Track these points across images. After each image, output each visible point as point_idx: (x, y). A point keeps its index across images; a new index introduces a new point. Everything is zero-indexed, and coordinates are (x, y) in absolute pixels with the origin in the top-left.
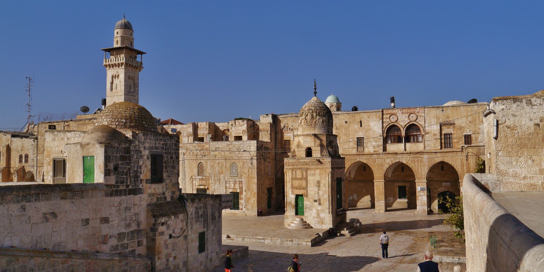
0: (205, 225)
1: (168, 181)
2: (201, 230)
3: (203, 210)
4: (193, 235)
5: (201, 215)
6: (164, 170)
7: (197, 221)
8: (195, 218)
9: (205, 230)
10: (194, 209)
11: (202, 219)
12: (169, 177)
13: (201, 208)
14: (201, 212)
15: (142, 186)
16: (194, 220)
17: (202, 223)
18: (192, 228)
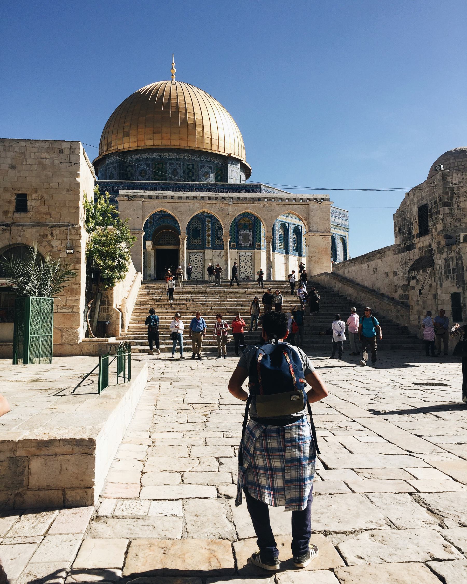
0: (460, 283)
1: (433, 230)
2: (455, 290)
3: (455, 261)
4: (444, 295)
5: (454, 269)
6: (429, 219)
7: (447, 277)
8: (445, 273)
9: (461, 290)
10: (443, 261)
11: (455, 275)
12: (434, 225)
13: (452, 259)
14: (452, 265)
15: (414, 241)
16: (444, 276)
17: (455, 281)
18: (441, 286)
